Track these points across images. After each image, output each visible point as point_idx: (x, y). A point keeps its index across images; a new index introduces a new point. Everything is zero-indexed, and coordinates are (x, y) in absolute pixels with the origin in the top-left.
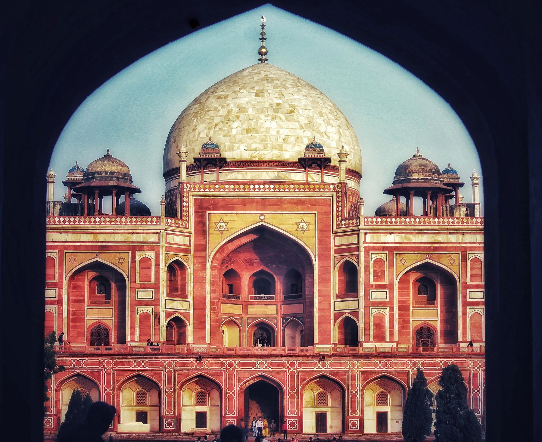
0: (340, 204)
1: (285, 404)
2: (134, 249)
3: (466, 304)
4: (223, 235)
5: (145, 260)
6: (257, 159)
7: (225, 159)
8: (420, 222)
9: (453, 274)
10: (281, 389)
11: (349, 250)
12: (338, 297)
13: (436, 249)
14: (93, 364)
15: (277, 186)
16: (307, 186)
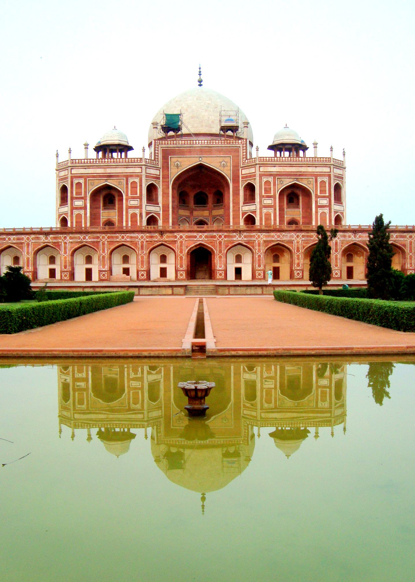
0: (245, 151)
1: (216, 261)
2: (127, 177)
3: (317, 207)
4: (179, 170)
5: (134, 183)
6: (197, 132)
7: (179, 129)
8: (291, 160)
9: (310, 189)
10: (214, 252)
11: (250, 176)
12: (244, 203)
13: (300, 175)
14: (94, 238)
15: (209, 142)
16: (226, 141)
